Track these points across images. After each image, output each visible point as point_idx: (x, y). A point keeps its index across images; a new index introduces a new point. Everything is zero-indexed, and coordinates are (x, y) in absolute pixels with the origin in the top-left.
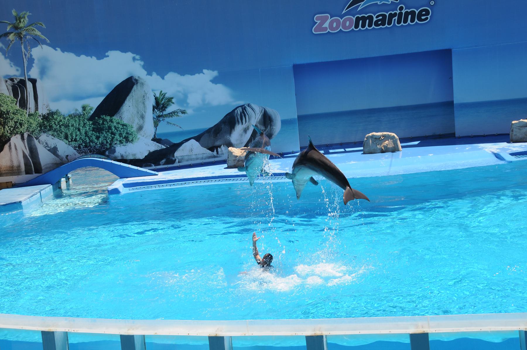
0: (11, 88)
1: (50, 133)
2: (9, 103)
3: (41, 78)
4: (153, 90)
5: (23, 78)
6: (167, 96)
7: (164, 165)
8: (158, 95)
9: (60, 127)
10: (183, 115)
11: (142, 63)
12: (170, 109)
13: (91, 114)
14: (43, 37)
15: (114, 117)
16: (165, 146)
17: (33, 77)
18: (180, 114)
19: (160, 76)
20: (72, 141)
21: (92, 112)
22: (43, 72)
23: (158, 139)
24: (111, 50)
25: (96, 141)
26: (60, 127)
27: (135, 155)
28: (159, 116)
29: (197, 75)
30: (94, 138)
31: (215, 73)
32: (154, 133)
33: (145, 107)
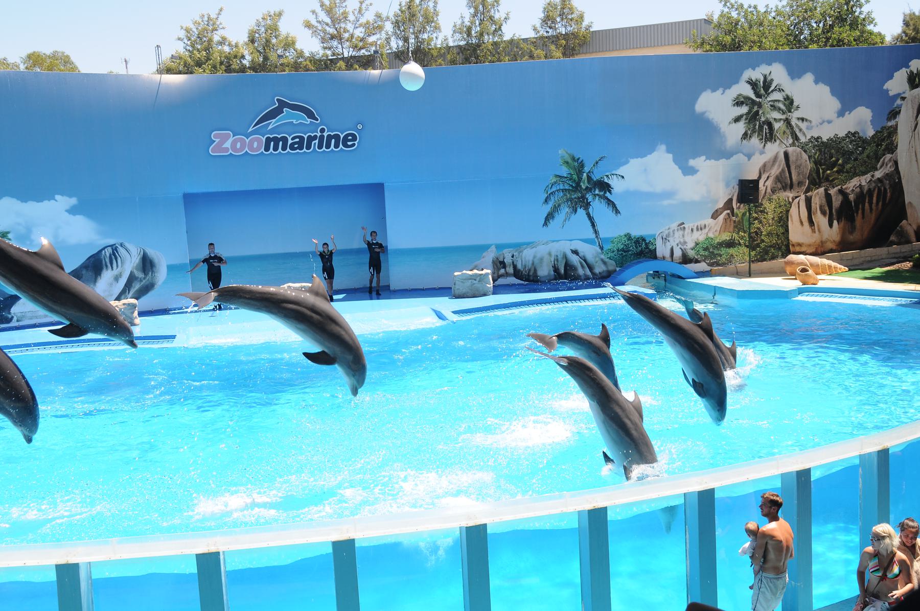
29: (46, 202)
31: (73, 201)
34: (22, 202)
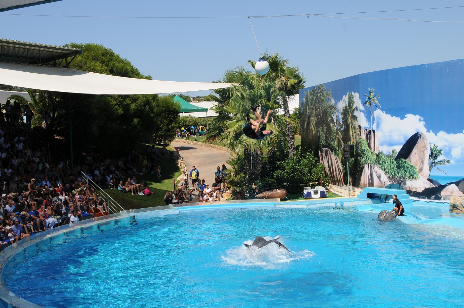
0: (366, 135)
1: (379, 165)
2: (365, 144)
3: (377, 131)
4: (430, 143)
5: (370, 130)
6: (438, 148)
7: (433, 199)
8: (432, 147)
9: (383, 163)
10: (448, 164)
11: (424, 123)
12: (440, 158)
13: (396, 156)
14: (379, 104)
15: (406, 160)
16: (435, 186)
17: (374, 129)
18: (446, 163)
19: (435, 133)
20: (387, 173)
21: (397, 155)
22: (378, 126)
23: (431, 180)
24: (408, 113)
25: (397, 174)
26: (383, 163)
27: (416, 188)
28: (432, 163)
29: (458, 134)
30: (397, 172)
32: (429, 175)
33: (424, 155)
34: (448, 134)
